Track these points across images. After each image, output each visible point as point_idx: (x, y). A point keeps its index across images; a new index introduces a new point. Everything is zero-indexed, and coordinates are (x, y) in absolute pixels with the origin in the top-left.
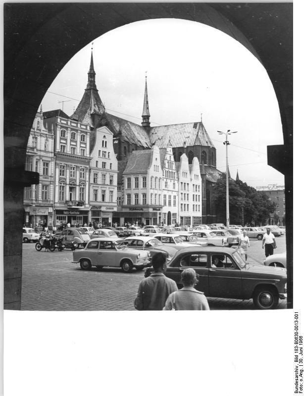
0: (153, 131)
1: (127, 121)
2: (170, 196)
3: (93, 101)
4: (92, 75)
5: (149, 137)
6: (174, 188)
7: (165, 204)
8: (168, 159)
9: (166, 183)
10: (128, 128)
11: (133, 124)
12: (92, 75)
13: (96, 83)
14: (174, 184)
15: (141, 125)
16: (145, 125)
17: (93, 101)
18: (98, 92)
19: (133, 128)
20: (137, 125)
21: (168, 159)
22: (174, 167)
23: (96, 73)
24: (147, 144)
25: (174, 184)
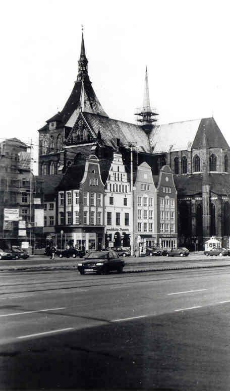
0: (154, 131)
1: (116, 121)
2: (118, 214)
3: (83, 97)
4: (84, 62)
5: (149, 139)
6: (125, 204)
7: (109, 223)
8: (115, 169)
9: (111, 199)
10: (116, 129)
11: (127, 124)
12: (84, 62)
13: (89, 74)
14: (125, 200)
15: (140, 124)
16: (145, 123)
17: (83, 97)
18: (92, 84)
19: (124, 129)
20: (131, 124)
21: (115, 169)
22: (125, 178)
23: (88, 60)
24: (142, 147)
25: (125, 200)
